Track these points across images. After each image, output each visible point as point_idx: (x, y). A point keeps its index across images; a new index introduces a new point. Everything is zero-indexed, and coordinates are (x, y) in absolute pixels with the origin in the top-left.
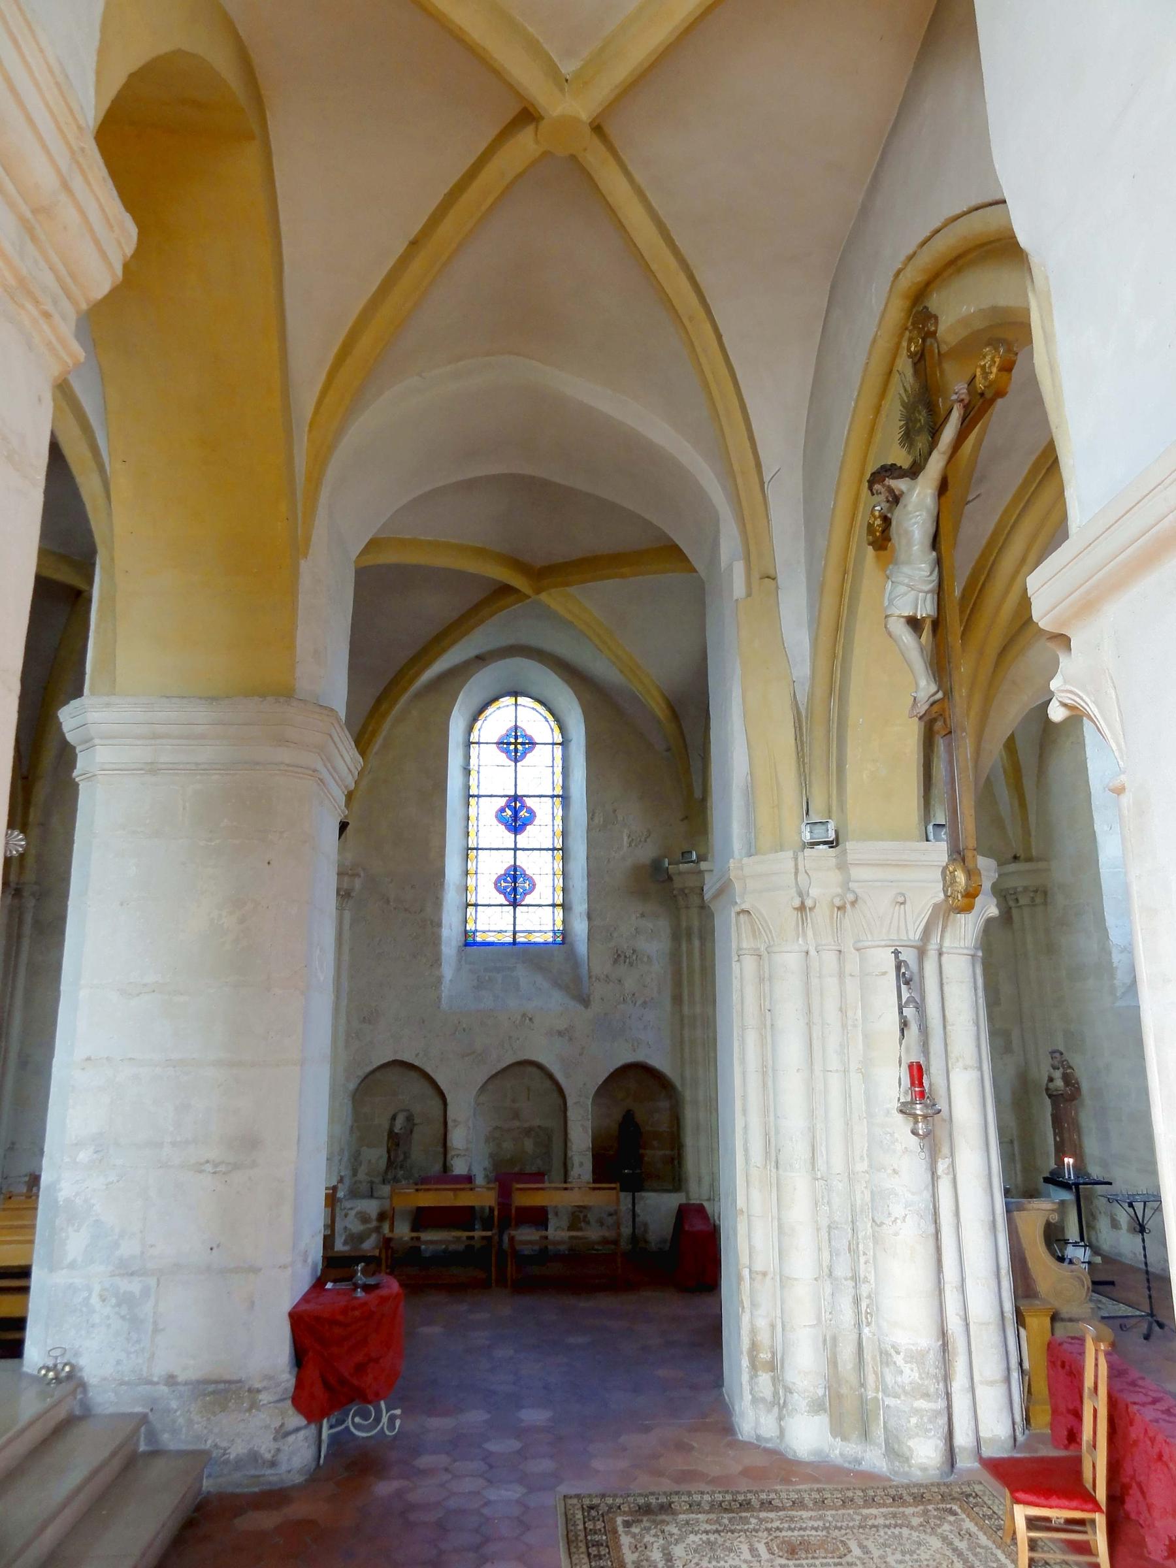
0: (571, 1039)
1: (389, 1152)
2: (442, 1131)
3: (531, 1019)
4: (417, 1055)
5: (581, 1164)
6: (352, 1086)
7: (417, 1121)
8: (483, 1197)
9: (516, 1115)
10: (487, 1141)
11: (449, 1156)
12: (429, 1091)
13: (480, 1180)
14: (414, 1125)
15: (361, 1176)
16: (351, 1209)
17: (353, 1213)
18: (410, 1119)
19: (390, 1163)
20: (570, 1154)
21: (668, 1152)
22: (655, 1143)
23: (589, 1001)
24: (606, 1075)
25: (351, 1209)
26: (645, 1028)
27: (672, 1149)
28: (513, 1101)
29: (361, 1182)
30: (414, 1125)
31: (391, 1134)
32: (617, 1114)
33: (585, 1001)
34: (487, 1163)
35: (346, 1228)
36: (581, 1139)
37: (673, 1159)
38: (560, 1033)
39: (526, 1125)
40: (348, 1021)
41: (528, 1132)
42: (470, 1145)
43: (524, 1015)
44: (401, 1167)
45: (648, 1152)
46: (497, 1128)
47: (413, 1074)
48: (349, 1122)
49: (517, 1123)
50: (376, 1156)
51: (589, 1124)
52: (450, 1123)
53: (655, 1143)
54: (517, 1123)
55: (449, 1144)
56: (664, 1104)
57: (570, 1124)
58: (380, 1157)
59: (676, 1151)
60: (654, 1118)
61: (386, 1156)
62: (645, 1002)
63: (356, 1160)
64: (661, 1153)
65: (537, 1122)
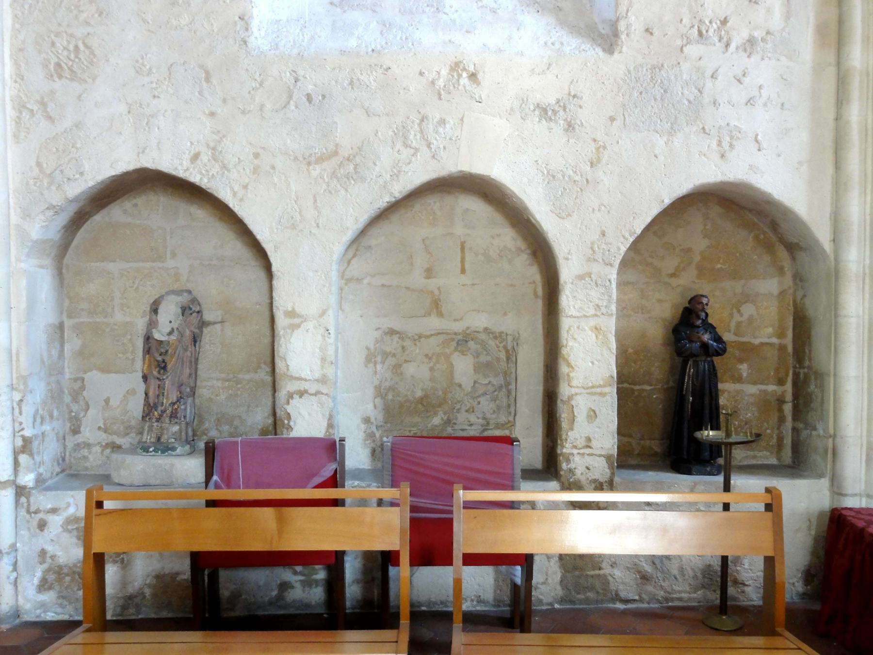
0: (570, 127)
1: (145, 378)
2: (267, 340)
3: (473, 76)
4: (196, 157)
5: (593, 415)
6: (43, 227)
7: (208, 316)
8: (371, 525)
9: (436, 306)
10: (370, 359)
11: (282, 395)
12: (235, 247)
13: (357, 456)
14: (203, 324)
15: (88, 433)
16: (54, 511)
17: (55, 522)
18: (190, 309)
19: (150, 408)
20: (564, 390)
21: (771, 388)
22: (744, 369)
23: (616, 34)
24: (655, 210)
25: (54, 511)
26: (750, 102)
27: (781, 382)
28: (429, 273)
29: (88, 446)
30: (203, 324)
31: (148, 338)
32: (664, 308)
33: (608, 38)
34: (370, 408)
35: (43, 553)
36: (591, 360)
37: (781, 401)
38: (545, 112)
39: (458, 327)
40: (19, 77)
41: (463, 341)
42: (329, 373)
43: (456, 67)
44: (174, 416)
46: (392, 332)
47: (200, 213)
48: (47, 312)
49: (434, 323)
50: (121, 390)
51: (611, 325)
52: (281, 321)
53: (744, 369)
54: (434, 323)
55: (280, 365)
57: (565, 323)
58: (132, 392)
59: (789, 387)
60: (748, 313)
61: (142, 387)
62: (751, 42)
63: (67, 401)
64: (752, 389)
65: (480, 322)
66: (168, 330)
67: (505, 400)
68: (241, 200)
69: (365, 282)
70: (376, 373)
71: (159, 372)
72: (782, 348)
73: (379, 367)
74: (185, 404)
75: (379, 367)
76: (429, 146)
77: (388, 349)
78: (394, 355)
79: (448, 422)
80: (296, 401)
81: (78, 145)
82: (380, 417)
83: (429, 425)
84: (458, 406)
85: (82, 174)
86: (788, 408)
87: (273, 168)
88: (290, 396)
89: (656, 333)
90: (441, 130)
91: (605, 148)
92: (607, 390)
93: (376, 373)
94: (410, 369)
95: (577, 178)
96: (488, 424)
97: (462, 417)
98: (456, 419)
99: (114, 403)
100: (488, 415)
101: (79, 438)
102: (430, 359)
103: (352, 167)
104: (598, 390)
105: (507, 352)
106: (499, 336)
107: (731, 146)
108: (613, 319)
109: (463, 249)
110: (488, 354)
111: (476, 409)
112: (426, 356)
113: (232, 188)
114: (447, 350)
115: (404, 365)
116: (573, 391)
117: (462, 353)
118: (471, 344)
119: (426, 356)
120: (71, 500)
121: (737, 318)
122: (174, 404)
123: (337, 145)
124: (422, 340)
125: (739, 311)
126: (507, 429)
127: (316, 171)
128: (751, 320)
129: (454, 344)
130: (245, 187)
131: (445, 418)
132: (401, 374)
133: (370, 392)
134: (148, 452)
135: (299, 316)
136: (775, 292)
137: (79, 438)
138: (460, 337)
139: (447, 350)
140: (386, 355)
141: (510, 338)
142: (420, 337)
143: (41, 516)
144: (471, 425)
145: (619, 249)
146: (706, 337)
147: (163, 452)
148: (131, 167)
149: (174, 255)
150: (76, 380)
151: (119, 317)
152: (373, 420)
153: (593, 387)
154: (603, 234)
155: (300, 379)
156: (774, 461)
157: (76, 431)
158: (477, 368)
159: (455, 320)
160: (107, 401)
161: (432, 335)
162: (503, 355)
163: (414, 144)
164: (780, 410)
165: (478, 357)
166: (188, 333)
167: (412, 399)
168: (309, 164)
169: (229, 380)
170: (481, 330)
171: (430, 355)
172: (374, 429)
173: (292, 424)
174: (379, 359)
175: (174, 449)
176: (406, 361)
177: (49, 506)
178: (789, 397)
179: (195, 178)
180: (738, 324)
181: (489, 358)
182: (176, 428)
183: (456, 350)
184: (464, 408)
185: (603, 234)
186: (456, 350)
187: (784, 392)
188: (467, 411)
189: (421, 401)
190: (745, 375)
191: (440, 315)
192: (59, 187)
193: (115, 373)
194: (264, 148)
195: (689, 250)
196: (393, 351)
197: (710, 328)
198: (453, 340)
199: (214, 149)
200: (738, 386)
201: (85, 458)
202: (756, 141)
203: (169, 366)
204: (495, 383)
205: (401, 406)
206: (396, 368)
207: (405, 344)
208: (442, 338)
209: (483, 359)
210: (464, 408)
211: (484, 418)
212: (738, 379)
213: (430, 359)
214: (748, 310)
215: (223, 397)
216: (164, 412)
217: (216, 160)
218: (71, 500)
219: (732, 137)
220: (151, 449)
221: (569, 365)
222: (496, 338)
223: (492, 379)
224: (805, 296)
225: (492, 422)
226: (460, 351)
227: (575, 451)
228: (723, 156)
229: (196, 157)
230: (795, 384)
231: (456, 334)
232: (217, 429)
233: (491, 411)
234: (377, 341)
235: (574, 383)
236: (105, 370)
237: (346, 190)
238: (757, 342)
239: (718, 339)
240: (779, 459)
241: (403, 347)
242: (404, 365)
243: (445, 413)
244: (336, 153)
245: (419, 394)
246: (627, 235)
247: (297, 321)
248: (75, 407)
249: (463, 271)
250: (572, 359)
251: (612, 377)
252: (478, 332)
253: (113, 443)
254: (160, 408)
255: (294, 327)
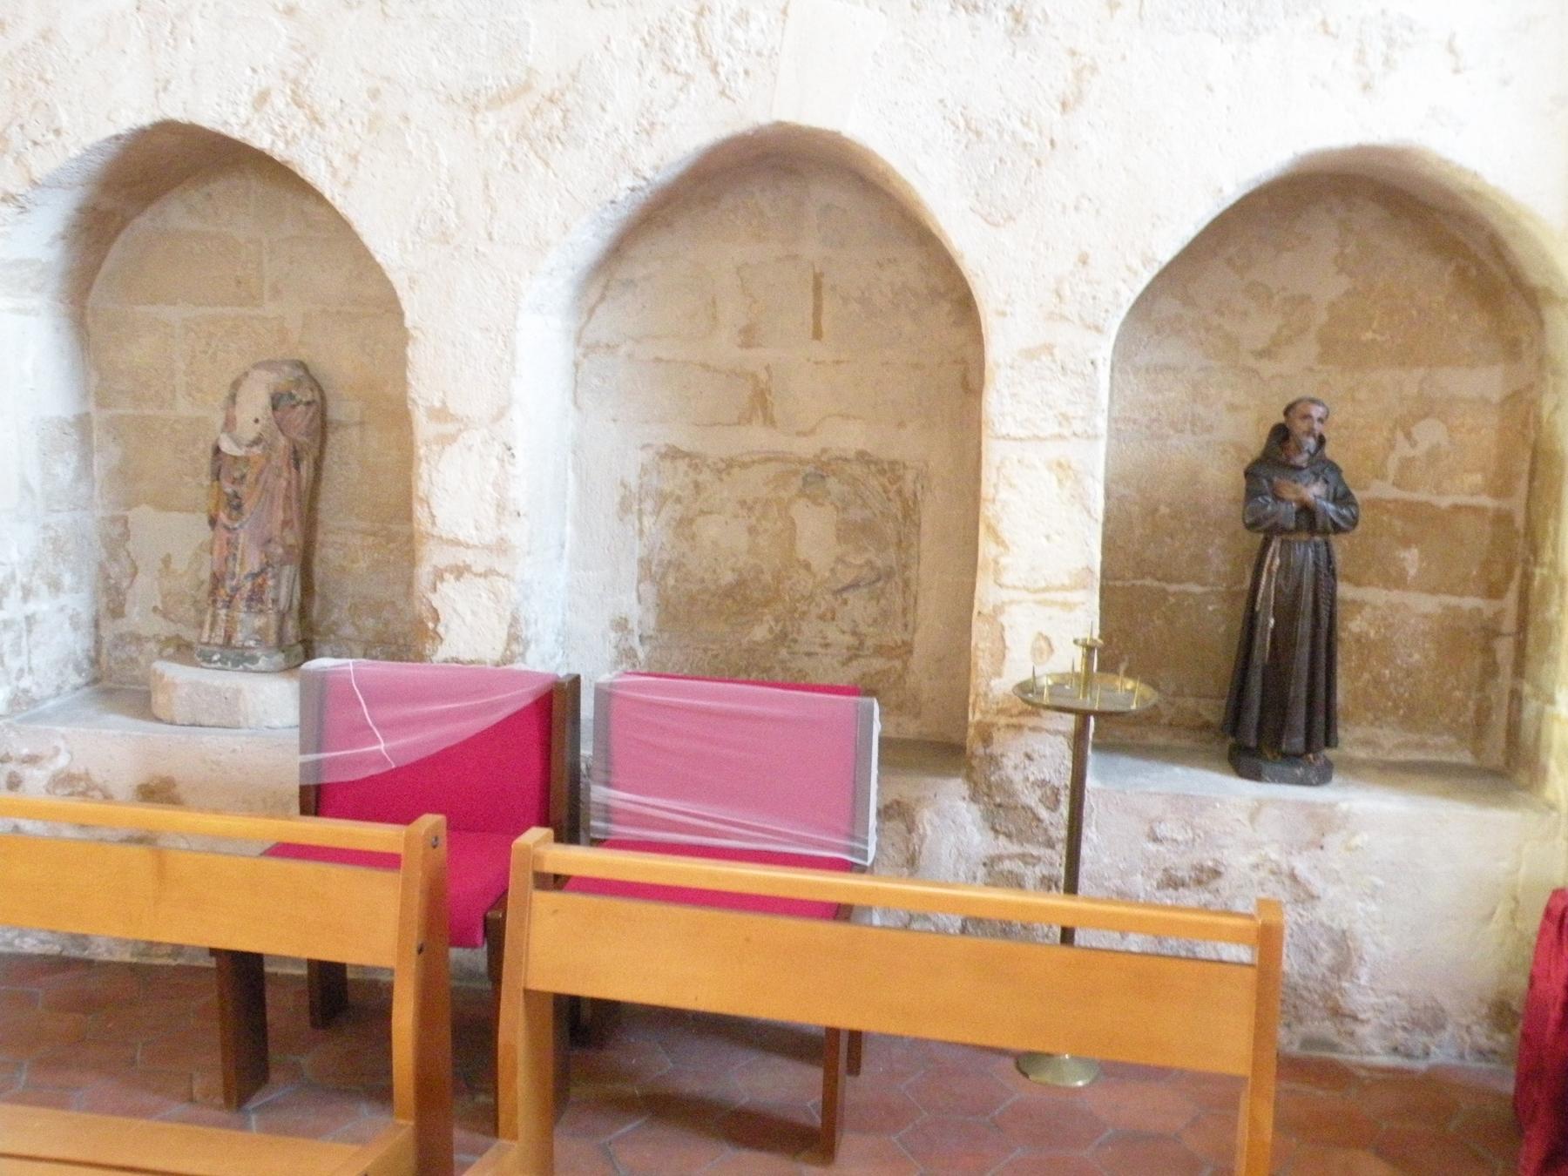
4: (262, 98)
9: (760, 403)
15: (137, 617)
16: (32, 760)
21: (1469, 602)
22: (1411, 559)
25: (32, 760)
28: (749, 336)
29: (138, 639)
37: (1491, 632)
39: (805, 448)
41: (816, 476)
45: (1376, 596)
46: (673, 454)
49: (757, 438)
51: (1094, 463)
53: (1411, 559)
54: (757, 438)
56: (1480, 382)
59: (1511, 598)
64: (1429, 604)
65: (850, 438)
66: (252, 436)
67: (898, 600)
68: (347, 184)
69: (623, 350)
70: (641, 532)
71: (229, 517)
72: (1502, 519)
73: (648, 521)
74: (276, 576)
75: (648, 521)
76: (714, 69)
77: (667, 488)
78: (679, 500)
79: (782, 638)
80: (449, 587)
81: (49, 76)
82: (651, 621)
83: (745, 641)
84: (802, 607)
85: (57, 132)
86: (1504, 649)
87: (406, 119)
88: (439, 575)
89: (1222, 478)
90: (739, 34)
91: (1094, 69)
92: (1077, 596)
93: (641, 532)
94: (710, 530)
95: (1031, 137)
96: (861, 643)
97: (809, 631)
98: (799, 631)
99: (179, 566)
100: (863, 629)
101: (122, 626)
102: (750, 509)
103: (557, 116)
104: (1060, 596)
105: (905, 501)
106: (891, 470)
107: (1387, 61)
108: (1101, 447)
109: (817, 288)
110: (865, 505)
111: (838, 615)
112: (743, 503)
113: (330, 163)
114: (783, 494)
115: (700, 520)
116: (1005, 595)
117: (815, 500)
118: (832, 483)
119: (743, 503)
120: (61, 744)
121: (1404, 449)
122: (255, 576)
123: (530, 71)
124: (736, 470)
125: (1408, 436)
126: (897, 657)
127: (489, 123)
128: (1433, 456)
129: (797, 482)
130: (354, 159)
131: (778, 629)
132: (693, 538)
133: (630, 571)
134: (210, 661)
135: (453, 418)
136: (1496, 397)
137: (122, 626)
138: (809, 469)
139: (783, 494)
140: (662, 498)
141: (910, 476)
142: (730, 464)
143: (10, 767)
144: (827, 646)
145: (1117, 293)
146: (1314, 492)
147: (236, 664)
148: (145, 120)
149: (276, 292)
150: (113, 520)
151: (183, 407)
152: (633, 624)
153: (1046, 589)
154: (1084, 260)
155: (456, 543)
156: (1466, 758)
157: (117, 612)
158: (850, 532)
159: (798, 434)
160: (167, 561)
161: (753, 462)
162: (896, 508)
163: (684, 67)
164: (1488, 650)
165: (845, 509)
166: (282, 441)
167: (713, 587)
168: (475, 109)
169: (374, 534)
170: (851, 454)
171: (749, 502)
172: (635, 642)
173: (441, 629)
174: (648, 505)
175: (254, 659)
176: (702, 513)
177: (25, 751)
178: (1509, 625)
179: (261, 140)
180: (1406, 464)
181: (868, 513)
182: (259, 622)
183: (802, 493)
184: (814, 611)
185: (1084, 260)
186: (802, 493)
187: (1499, 615)
188: (822, 617)
189: (729, 593)
190: (1412, 572)
191: (770, 421)
192: (18, 159)
193: (179, 510)
194: (388, 79)
195: (1304, 300)
196: (678, 492)
197: (1324, 467)
198: (796, 473)
199: (296, 82)
200: (1395, 596)
201: (133, 661)
202: (1451, 49)
203: (246, 507)
204: (879, 563)
205: (692, 600)
206: (684, 524)
207: (701, 478)
208: (773, 468)
209: (856, 514)
210: (814, 611)
211: (854, 633)
212: (1397, 581)
213: (750, 509)
214: (1430, 434)
215: (363, 565)
216: (236, 589)
217: (300, 105)
218: (61, 744)
219: (1390, 42)
220: (215, 658)
221: (999, 541)
222: (882, 472)
223: (871, 554)
224: (1557, 407)
225: (869, 642)
226: (808, 497)
227: (1002, 720)
228: (1366, 87)
229: (262, 98)
230: (1524, 598)
231: (801, 462)
232: (353, 624)
233: (870, 621)
234: (644, 470)
235: (1006, 579)
236: (162, 505)
237: (547, 164)
238: (1445, 502)
239: (1343, 498)
240: (1476, 753)
241: (697, 485)
242: (700, 520)
243: (777, 620)
244: (527, 87)
245: (728, 577)
246: (1136, 263)
247: (450, 428)
248: (115, 570)
249: (817, 334)
250: (1005, 529)
251: (1089, 570)
252: (846, 460)
253: (178, 637)
254: (230, 583)
255: (446, 440)
